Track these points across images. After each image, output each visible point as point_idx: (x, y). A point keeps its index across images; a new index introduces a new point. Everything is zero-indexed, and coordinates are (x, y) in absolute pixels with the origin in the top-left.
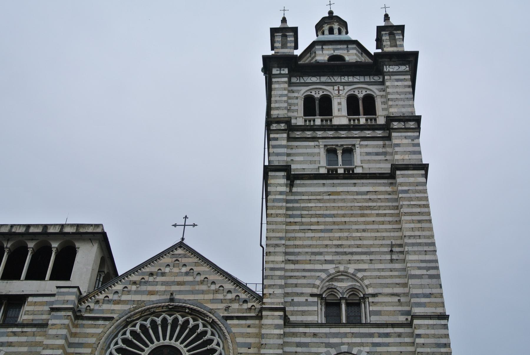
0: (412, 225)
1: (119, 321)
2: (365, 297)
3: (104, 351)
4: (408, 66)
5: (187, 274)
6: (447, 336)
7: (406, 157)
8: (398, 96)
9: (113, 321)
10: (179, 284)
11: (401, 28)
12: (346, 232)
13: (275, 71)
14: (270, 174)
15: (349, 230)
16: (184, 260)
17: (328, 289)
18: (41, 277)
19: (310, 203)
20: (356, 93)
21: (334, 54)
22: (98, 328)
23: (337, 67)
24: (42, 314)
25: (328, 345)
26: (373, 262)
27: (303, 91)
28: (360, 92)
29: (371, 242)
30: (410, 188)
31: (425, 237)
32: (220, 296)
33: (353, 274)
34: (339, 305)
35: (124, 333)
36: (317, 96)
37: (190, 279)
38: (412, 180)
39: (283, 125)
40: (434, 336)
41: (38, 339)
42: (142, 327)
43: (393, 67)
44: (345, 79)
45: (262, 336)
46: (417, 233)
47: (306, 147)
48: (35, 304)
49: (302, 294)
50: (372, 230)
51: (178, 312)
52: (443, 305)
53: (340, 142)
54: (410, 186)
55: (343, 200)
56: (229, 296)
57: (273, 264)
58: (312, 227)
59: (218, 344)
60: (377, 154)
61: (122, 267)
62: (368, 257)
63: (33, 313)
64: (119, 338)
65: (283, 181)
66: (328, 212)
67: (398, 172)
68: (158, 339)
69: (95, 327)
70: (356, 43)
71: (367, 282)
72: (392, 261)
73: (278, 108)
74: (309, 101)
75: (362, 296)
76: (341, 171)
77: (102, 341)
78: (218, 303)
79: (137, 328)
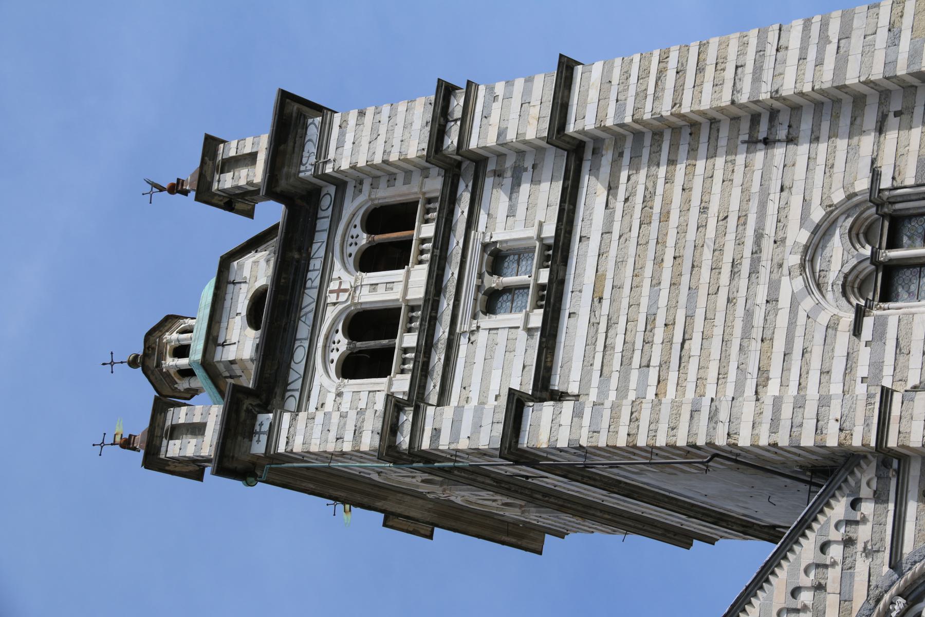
0: (708, 87)
4: (310, 121)
7: (534, 111)
8: (381, 140)
12: (701, 255)
13: (259, 448)
14: (525, 442)
17: (844, 294)
19: (613, 348)
20: (353, 250)
21: (244, 313)
23: (277, 313)
26: (787, 184)
27: (325, 380)
28: (353, 241)
29: (736, 192)
30: (613, 97)
31: (741, 53)
33: (814, 233)
36: (342, 344)
38: (593, 95)
39: (403, 417)
43: (305, 154)
44: (314, 277)
46: (729, 73)
47: (469, 363)
54: (607, 98)
55: (619, 263)
57: (760, 423)
58: (678, 338)
62: (775, 195)
65: (548, 408)
66: (644, 302)
67: (571, 129)
73: (358, 433)
74: (353, 367)
75: (874, 210)
76: (544, 276)
78: (852, 576)
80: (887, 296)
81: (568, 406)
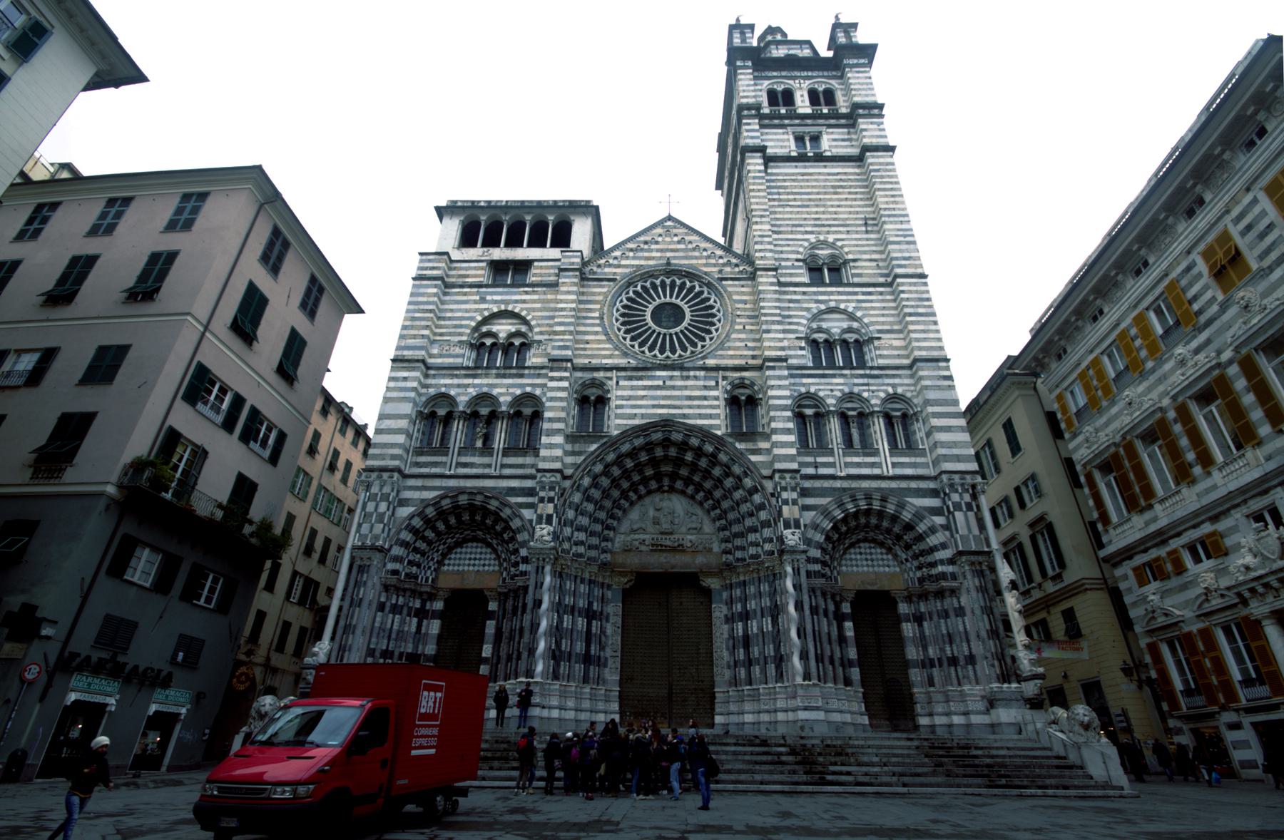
2: (846, 262)
5: (679, 242)
6: (928, 292)
10: (672, 250)
11: (855, 26)
13: (739, 63)
15: (824, 206)
16: (675, 231)
18: (542, 244)
25: (817, 301)
32: (713, 261)
34: (820, 270)
36: (780, 88)
37: (682, 246)
38: (881, 160)
40: (917, 292)
41: (549, 297)
42: (643, 287)
45: (760, 292)
48: (541, 268)
49: (787, 260)
50: (846, 206)
52: (921, 266)
53: (807, 129)
56: (721, 261)
60: (843, 140)
61: (608, 244)
63: (541, 275)
64: (624, 297)
65: (761, 161)
70: (809, 43)
71: (846, 249)
72: (867, 232)
74: (772, 95)
79: (639, 288)
80: (811, 270)
81: (762, 168)
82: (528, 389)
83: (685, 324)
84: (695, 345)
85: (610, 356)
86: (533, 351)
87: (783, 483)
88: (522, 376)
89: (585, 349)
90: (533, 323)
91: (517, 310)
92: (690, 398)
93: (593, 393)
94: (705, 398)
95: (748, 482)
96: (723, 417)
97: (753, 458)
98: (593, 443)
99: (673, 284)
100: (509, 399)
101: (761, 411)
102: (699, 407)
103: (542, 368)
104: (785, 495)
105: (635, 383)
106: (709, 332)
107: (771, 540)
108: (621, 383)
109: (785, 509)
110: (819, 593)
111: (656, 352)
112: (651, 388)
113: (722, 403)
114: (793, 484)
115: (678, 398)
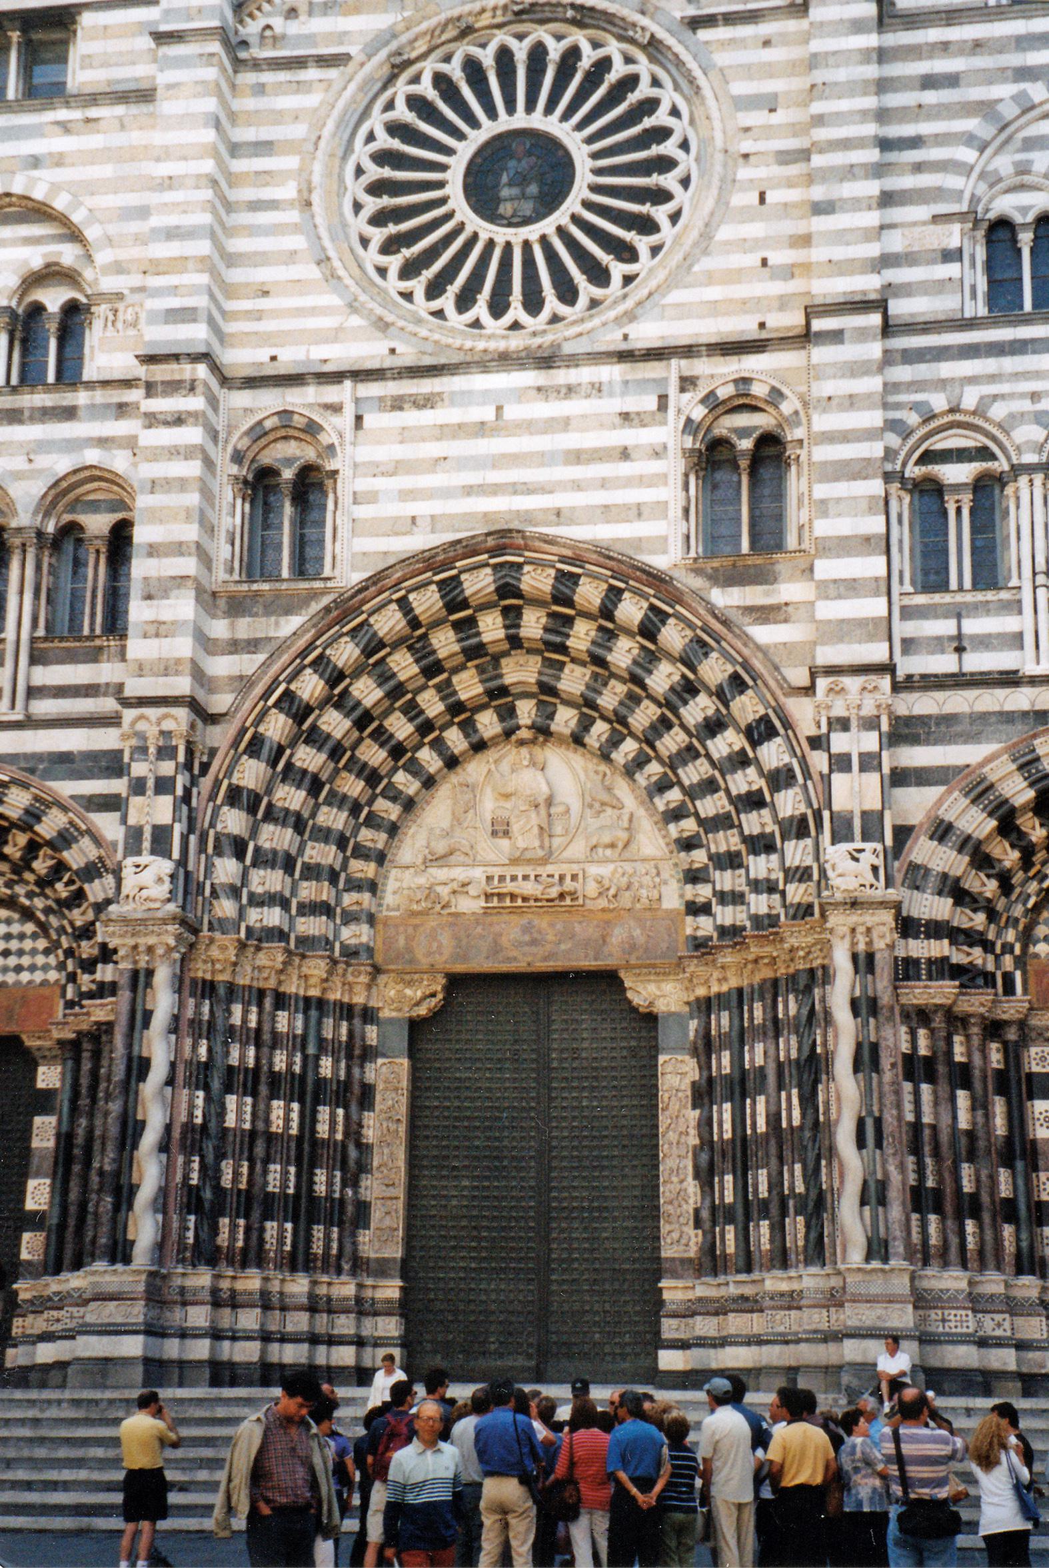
1: (368, 67)
3: (337, 162)
9: (352, 66)
22: (309, 92)
24: (134, 63)
35: (390, 106)
42: (441, 81)
51: (542, 22)
59: (675, 112)
68: (492, 113)
69: (297, 92)
77: (327, 132)
79: (426, 88)
82: (92, 456)
83: (573, 204)
84: (599, 276)
85: (336, 335)
86: (97, 324)
87: (839, 711)
88: (69, 413)
89: (258, 315)
90: (91, 233)
91: (38, 194)
92: (577, 457)
93: (287, 456)
94: (625, 454)
95: (747, 708)
96: (675, 511)
97: (763, 634)
98: (288, 611)
99: (538, 54)
100: (37, 488)
101: (795, 484)
102: (604, 484)
103: (128, 383)
104: (840, 742)
105: (411, 417)
106: (647, 226)
107: (802, 874)
108: (369, 420)
109: (838, 779)
110: (938, 1021)
111: (480, 309)
112: (459, 430)
113: (674, 466)
114: (868, 710)
115: (543, 459)
